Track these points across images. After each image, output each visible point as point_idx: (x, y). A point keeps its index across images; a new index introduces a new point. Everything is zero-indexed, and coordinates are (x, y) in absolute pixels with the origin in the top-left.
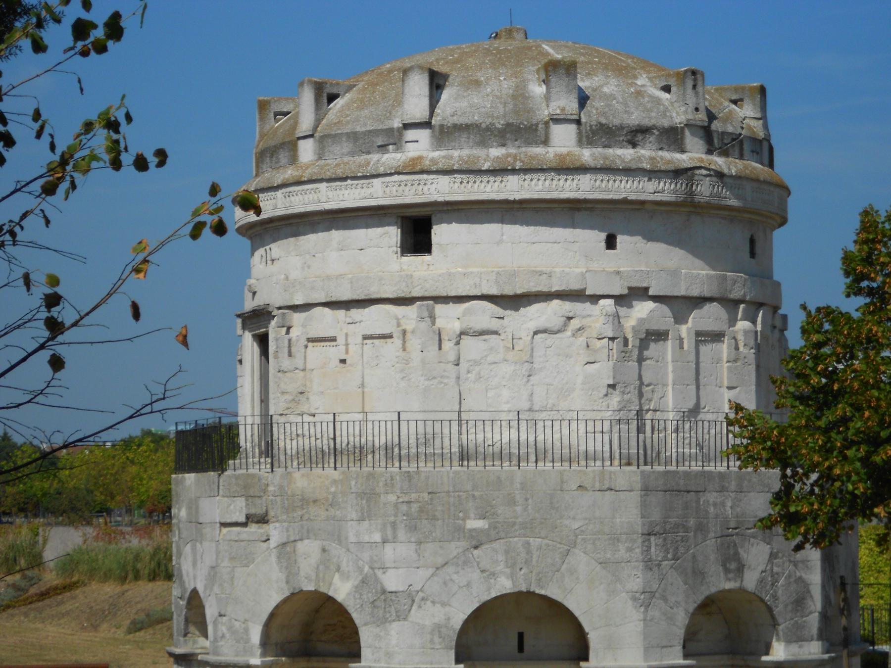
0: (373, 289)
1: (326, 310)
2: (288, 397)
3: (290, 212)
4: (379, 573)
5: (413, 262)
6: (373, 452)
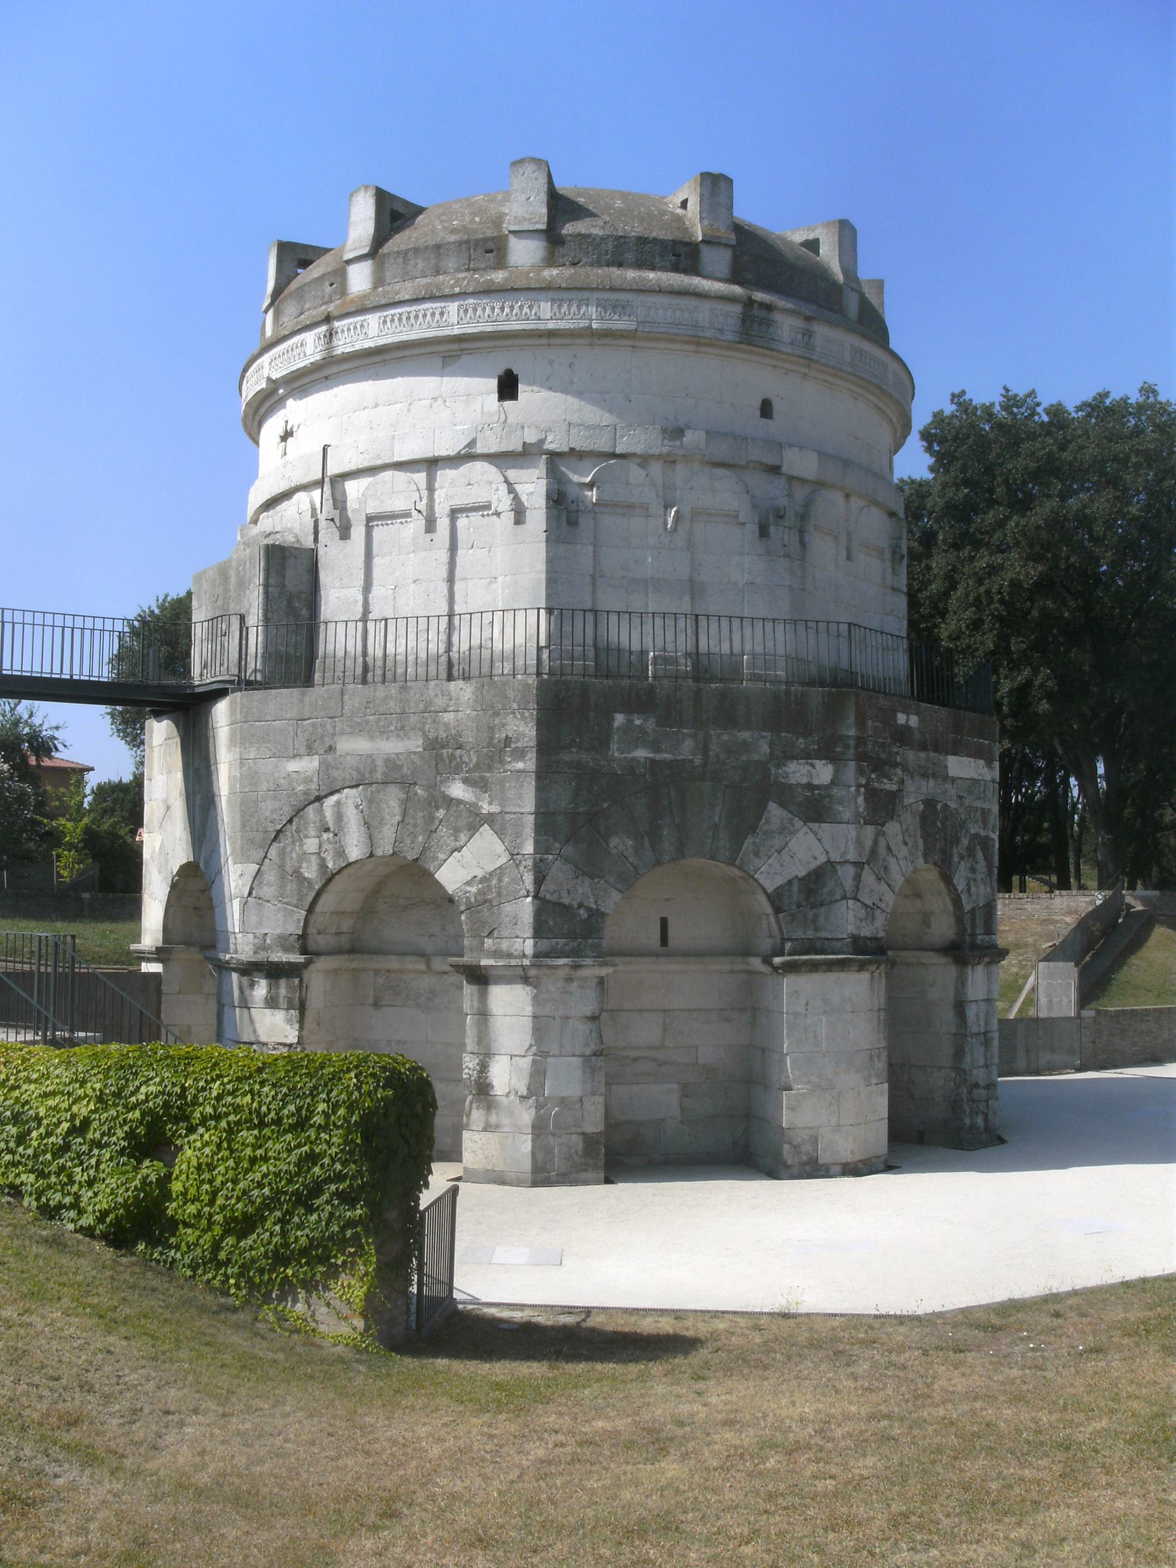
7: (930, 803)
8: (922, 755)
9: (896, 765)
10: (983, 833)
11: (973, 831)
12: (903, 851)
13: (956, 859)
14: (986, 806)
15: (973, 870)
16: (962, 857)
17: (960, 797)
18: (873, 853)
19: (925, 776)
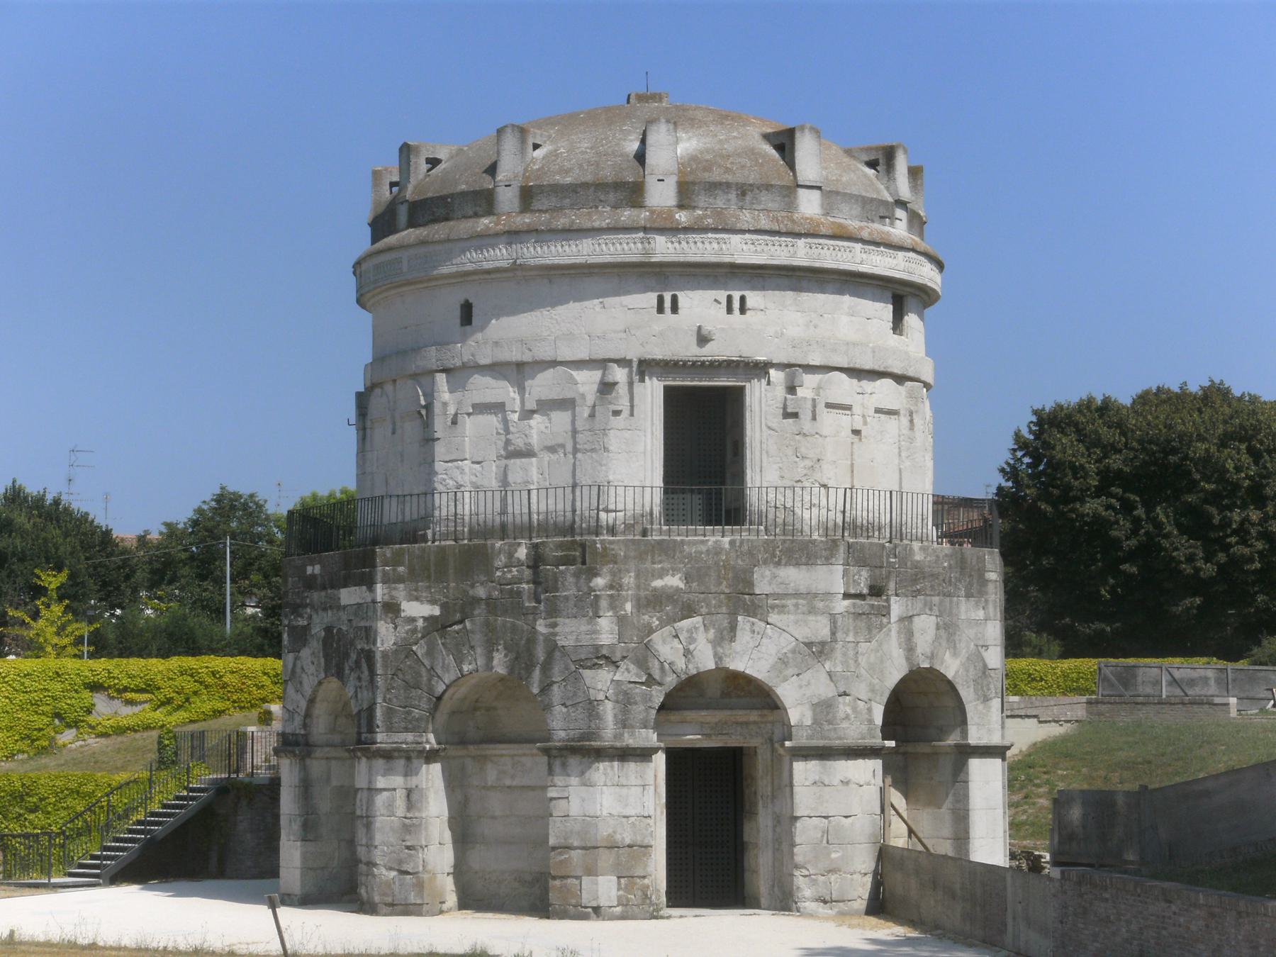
0: (890, 362)
1: (844, 376)
2: (808, 463)
3: (817, 265)
4: (982, 650)
5: (893, 340)
6: (879, 529)
7: (328, 630)
8: (323, 593)
9: (307, 606)
10: (367, 648)
11: (359, 647)
12: (312, 669)
13: (347, 672)
14: (368, 624)
15: (359, 679)
16: (352, 669)
17: (350, 621)
18: (293, 671)
19: (325, 609)
